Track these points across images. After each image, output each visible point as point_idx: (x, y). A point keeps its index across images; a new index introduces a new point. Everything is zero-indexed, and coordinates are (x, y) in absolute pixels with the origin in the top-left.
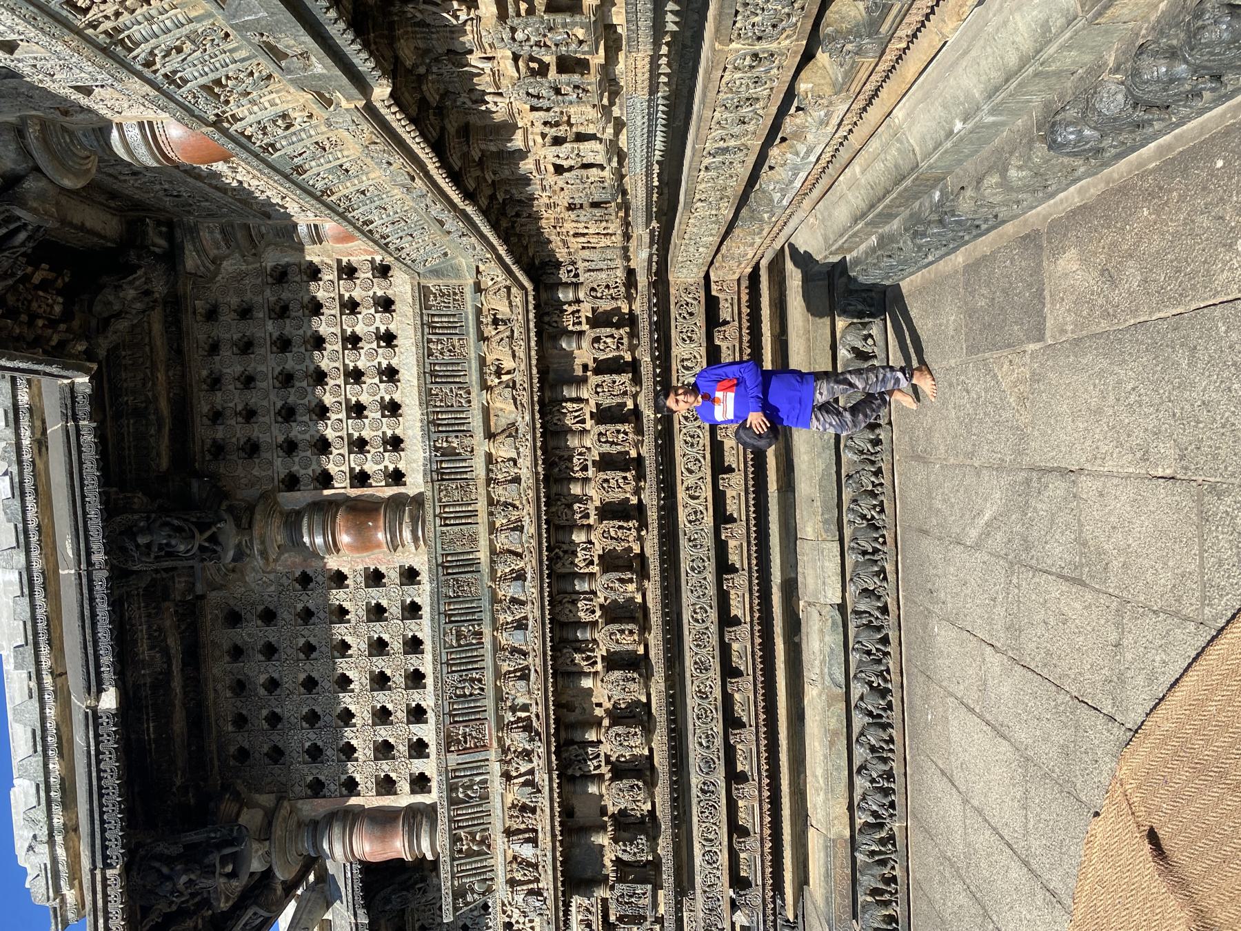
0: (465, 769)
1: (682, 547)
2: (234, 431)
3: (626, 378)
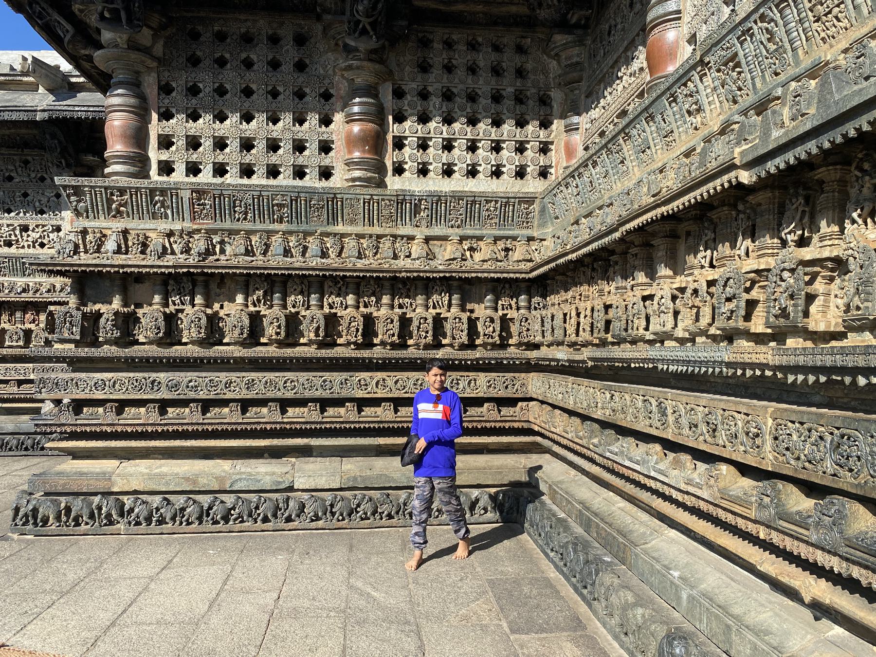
1: (341, 374)
2: (438, 57)
3: (465, 339)
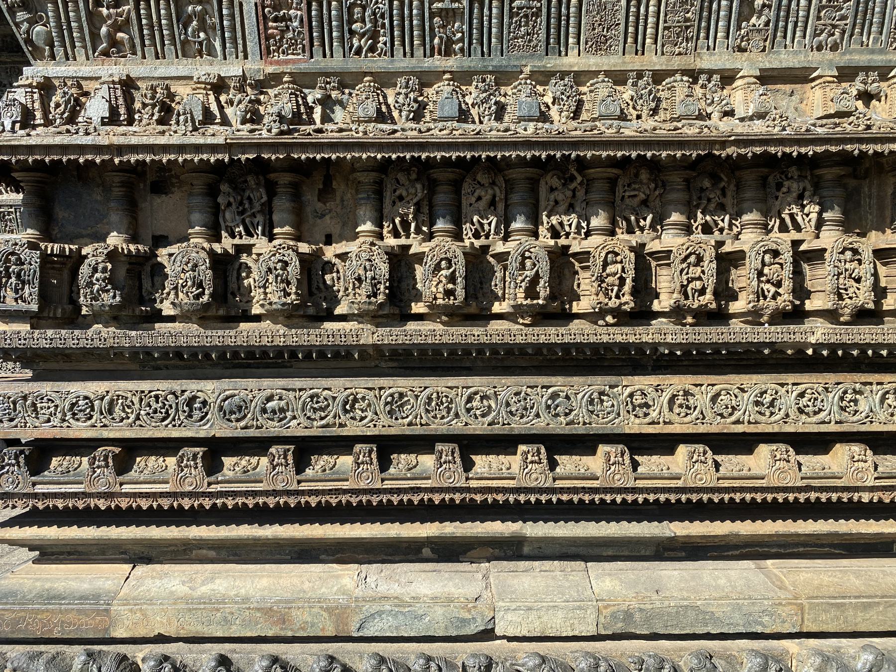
0: (232, 16)
1: (590, 379)
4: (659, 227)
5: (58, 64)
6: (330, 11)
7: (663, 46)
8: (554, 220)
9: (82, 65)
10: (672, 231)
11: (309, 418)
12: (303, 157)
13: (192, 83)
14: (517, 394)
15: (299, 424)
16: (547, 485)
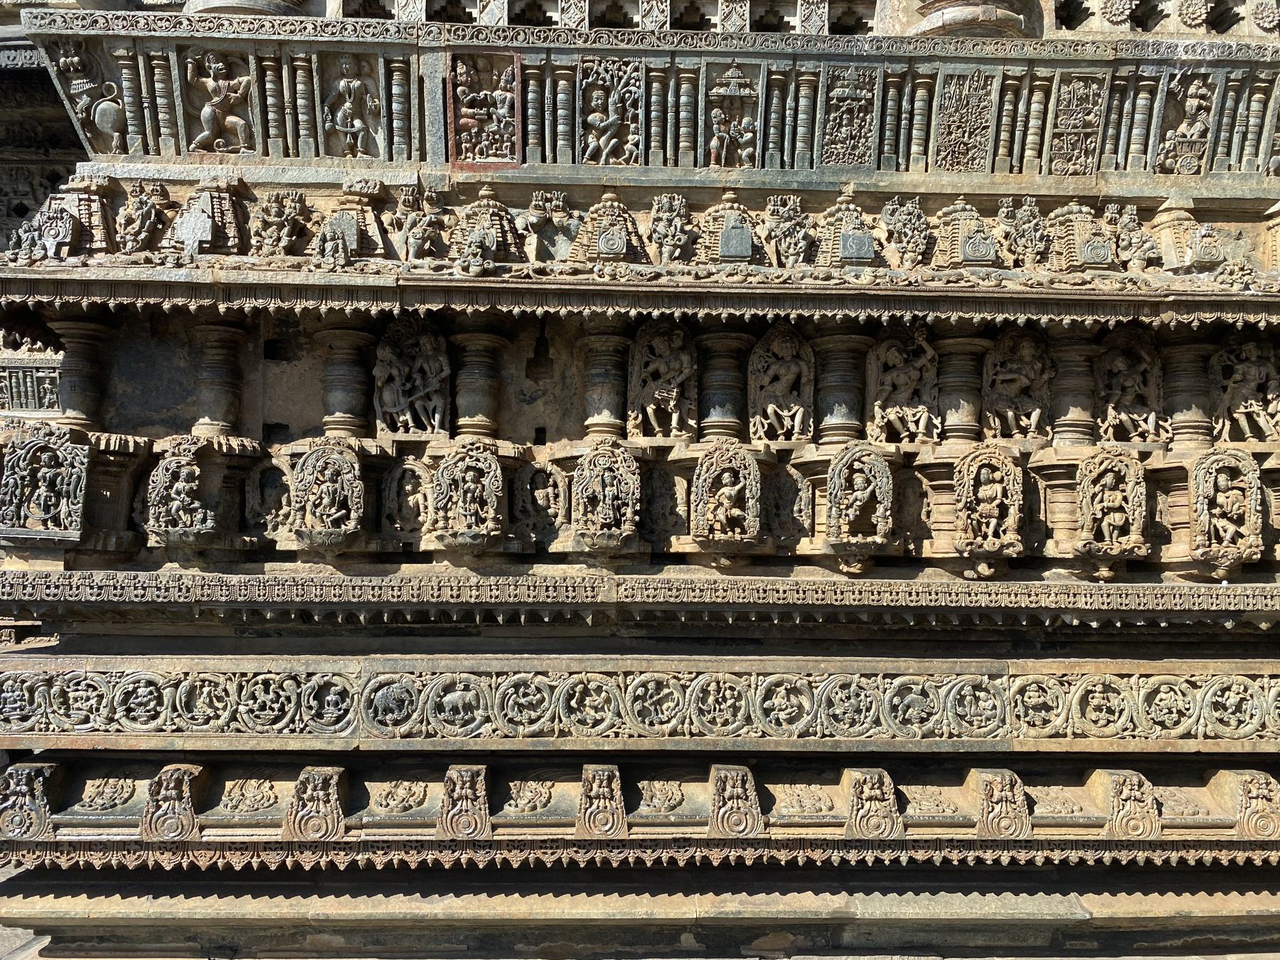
0: (407, 97)
4: (1048, 428)
5: (132, 160)
6: (555, 94)
7: (1051, 161)
8: (892, 414)
9: (168, 161)
10: (1070, 435)
11: (511, 721)
12: (516, 310)
13: (340, 192)
14: (845, 686)
15: (494, 731)
16: (894, 836)
